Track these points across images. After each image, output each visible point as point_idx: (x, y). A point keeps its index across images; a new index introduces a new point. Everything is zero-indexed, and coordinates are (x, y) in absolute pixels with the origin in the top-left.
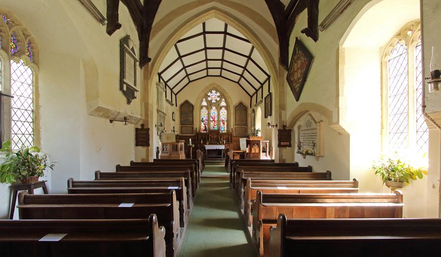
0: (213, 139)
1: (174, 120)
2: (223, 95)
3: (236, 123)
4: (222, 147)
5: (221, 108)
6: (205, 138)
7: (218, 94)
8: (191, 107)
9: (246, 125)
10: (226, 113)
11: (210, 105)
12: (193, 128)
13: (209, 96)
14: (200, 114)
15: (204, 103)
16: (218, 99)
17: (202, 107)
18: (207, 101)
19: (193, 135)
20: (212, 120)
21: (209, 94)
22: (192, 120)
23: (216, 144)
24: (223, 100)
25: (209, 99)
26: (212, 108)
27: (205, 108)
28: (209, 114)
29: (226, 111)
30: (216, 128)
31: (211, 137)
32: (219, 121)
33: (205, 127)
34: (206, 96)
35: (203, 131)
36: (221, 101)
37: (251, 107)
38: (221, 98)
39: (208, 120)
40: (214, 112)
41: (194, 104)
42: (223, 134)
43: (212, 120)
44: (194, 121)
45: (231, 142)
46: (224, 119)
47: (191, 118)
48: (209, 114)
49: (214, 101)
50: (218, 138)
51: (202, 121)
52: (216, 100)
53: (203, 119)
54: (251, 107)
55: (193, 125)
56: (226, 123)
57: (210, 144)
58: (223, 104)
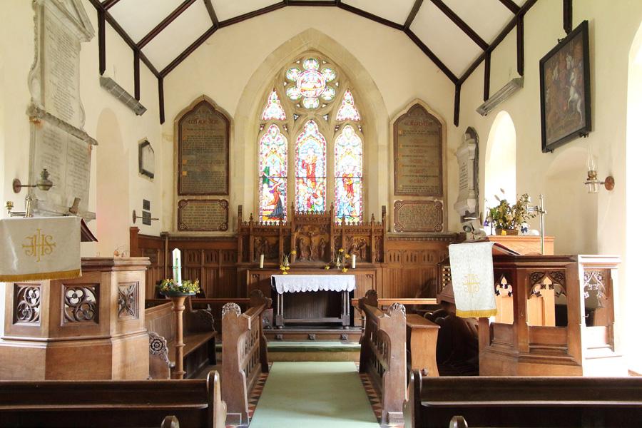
0: (309, 249)
1: (151, 176)
2: (348, 79)
4: (342, 282)
5: (338, 127)
6: (278, 242)
7: (329, 75)
9: (440, 191)
10: (359, 149)
11: (296, 115)
12: (226, 206)
13: (294, 84)
14: (257, 153)
15: (274, 111)
16: (329, 94)
17: (263, 125)
18: (283, 100)
19: (229, 233)
20: (303, 173)
21: (293, 75)
22: (224, 175)
23: (321, 270)
24: (348, 96)
25: (293, 93)
26: (301, 129)
27: (275, 130)
28: (291, 152)
29: (358, 140)
30: (319, 206)
31: (298, 241)
32: (329, 176)
33: (278, 202)
34: (281, 83)
35: (270, 217)
36: (338, 99)
37: (456, 122)
38: (339, 90)
39: (290, 177)
40: (310, 144)
41: (231, 112)
42: (349, 230)
43: (303, 173)
44: (233, 180)
45: (381, 260)
46: (349, 172)
47: (222, 169)
48: (291, 152)
49: (310, 103)
50: (328, 245)
52: (320, 98)
53: (267, 170)
54: (456, 122)
55: (227, 194)
56: (357, 188)
57: (294, 270)
58: (348, 111)
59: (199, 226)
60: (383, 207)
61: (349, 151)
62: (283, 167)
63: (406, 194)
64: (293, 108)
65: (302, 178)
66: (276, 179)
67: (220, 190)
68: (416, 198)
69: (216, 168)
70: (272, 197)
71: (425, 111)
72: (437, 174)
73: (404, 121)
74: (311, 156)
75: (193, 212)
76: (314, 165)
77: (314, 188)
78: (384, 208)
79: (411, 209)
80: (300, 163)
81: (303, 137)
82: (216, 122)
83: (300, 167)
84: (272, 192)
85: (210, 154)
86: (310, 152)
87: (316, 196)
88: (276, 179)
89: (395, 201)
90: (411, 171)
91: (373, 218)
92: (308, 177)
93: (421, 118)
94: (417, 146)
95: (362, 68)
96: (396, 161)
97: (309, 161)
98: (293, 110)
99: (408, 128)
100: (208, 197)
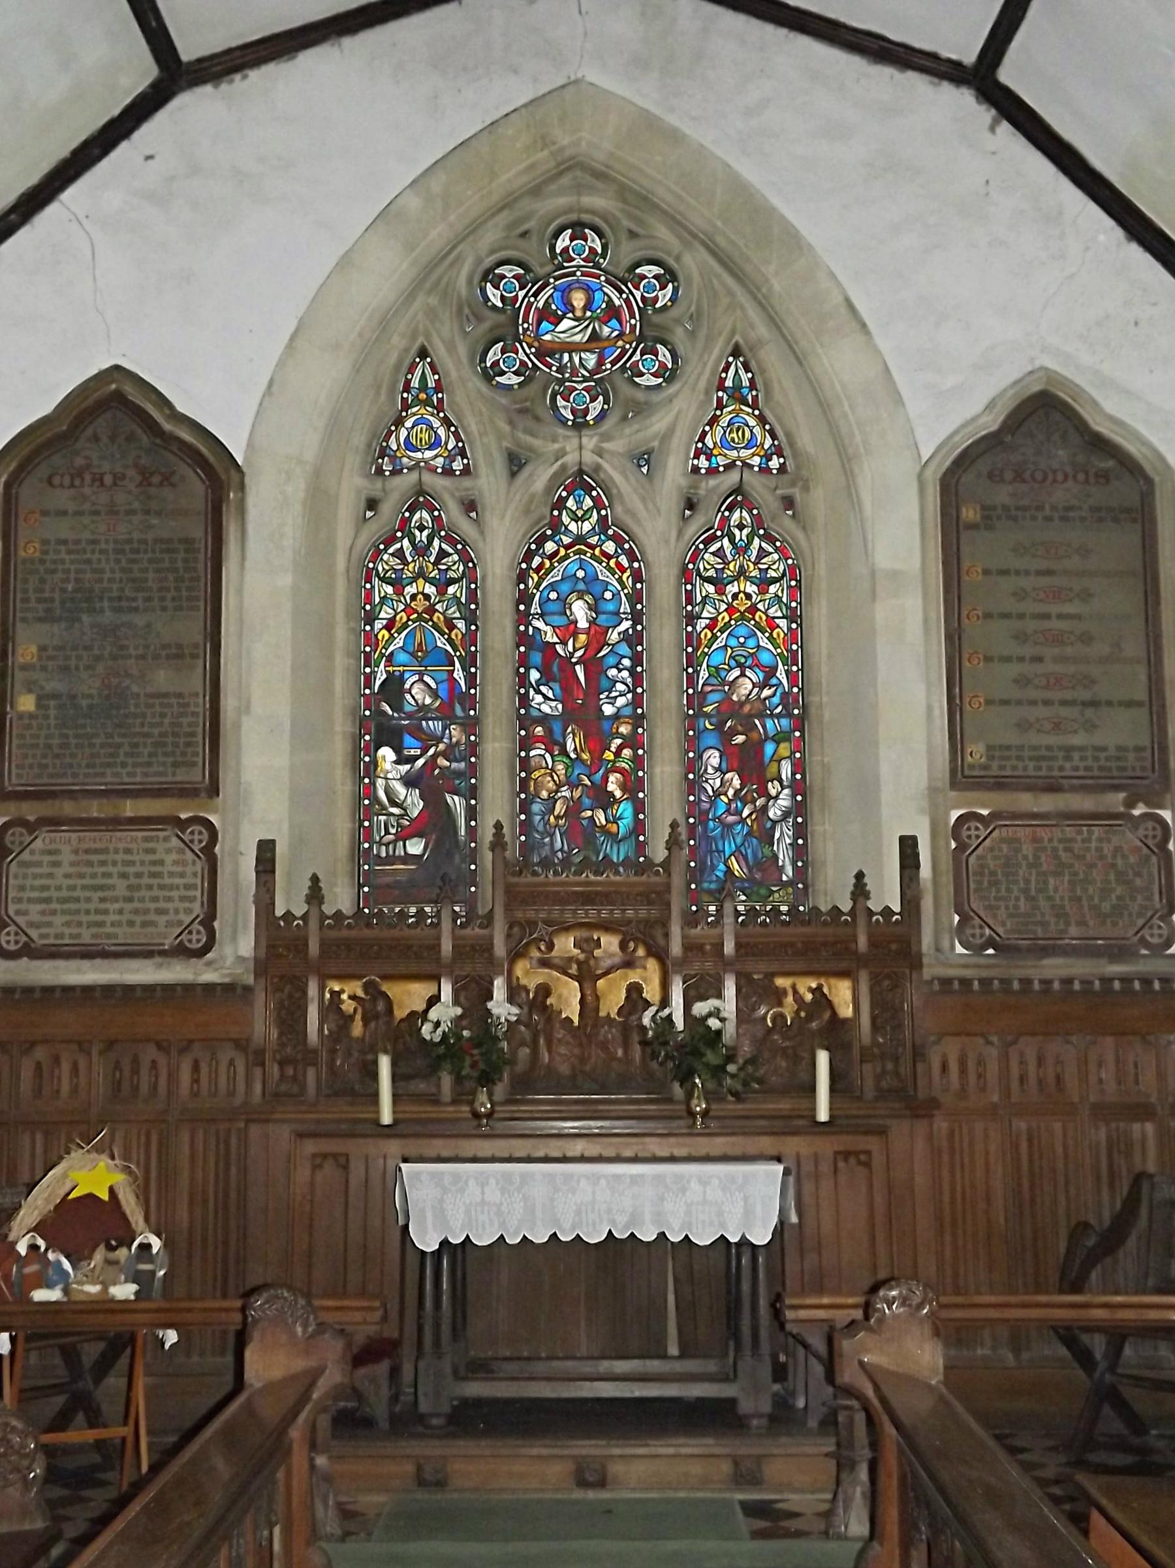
3: (976, 752)
8: (195, 486)
22: (201, 705)
47: (196, 681)
51: (389, 735)
53: (394, 688)
59: (86, 938)
60: (902, 839)
61: (742, 605)
62: (459, 674)
63: (1000, 784)
64: (506, 428)
65: (544, 719)
66: (435, 726)
67: (181, 776)
68: (1047, 803)
69: (162, 678)
70: (415, 803)
71: (1081, 426)
72: (1141, 694)
73: (983, 466)
74: (583, 624)
75: (59, 872)
76: (595, 667)
77: (598, 759)
78: (908, 845)
79: (1027, 849)
80: (537, 658)
81: (550, 547)
82: (167, 479)
83: (534, 675)
84: (409, 781)
85: (139, 620)
86: (580, 611)
87: (605, 801)
88: (435, 726)
89: (955, 815)
90: (1022, 681)
91: (860, 890)
92: (567, 717)
93: (1061, 452)
94: (1049, 573)
95: (793, 241)
96: (954, 639)
97: (574, 648)
98: (500, 437)
99: (1002, 495)
100: (129, 809)
